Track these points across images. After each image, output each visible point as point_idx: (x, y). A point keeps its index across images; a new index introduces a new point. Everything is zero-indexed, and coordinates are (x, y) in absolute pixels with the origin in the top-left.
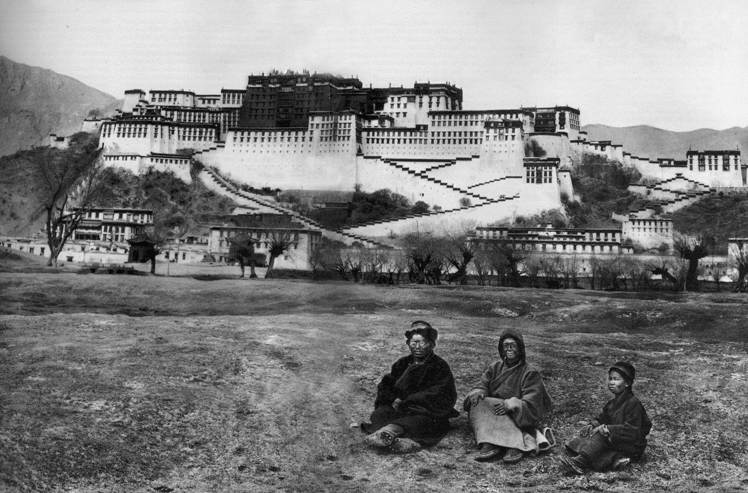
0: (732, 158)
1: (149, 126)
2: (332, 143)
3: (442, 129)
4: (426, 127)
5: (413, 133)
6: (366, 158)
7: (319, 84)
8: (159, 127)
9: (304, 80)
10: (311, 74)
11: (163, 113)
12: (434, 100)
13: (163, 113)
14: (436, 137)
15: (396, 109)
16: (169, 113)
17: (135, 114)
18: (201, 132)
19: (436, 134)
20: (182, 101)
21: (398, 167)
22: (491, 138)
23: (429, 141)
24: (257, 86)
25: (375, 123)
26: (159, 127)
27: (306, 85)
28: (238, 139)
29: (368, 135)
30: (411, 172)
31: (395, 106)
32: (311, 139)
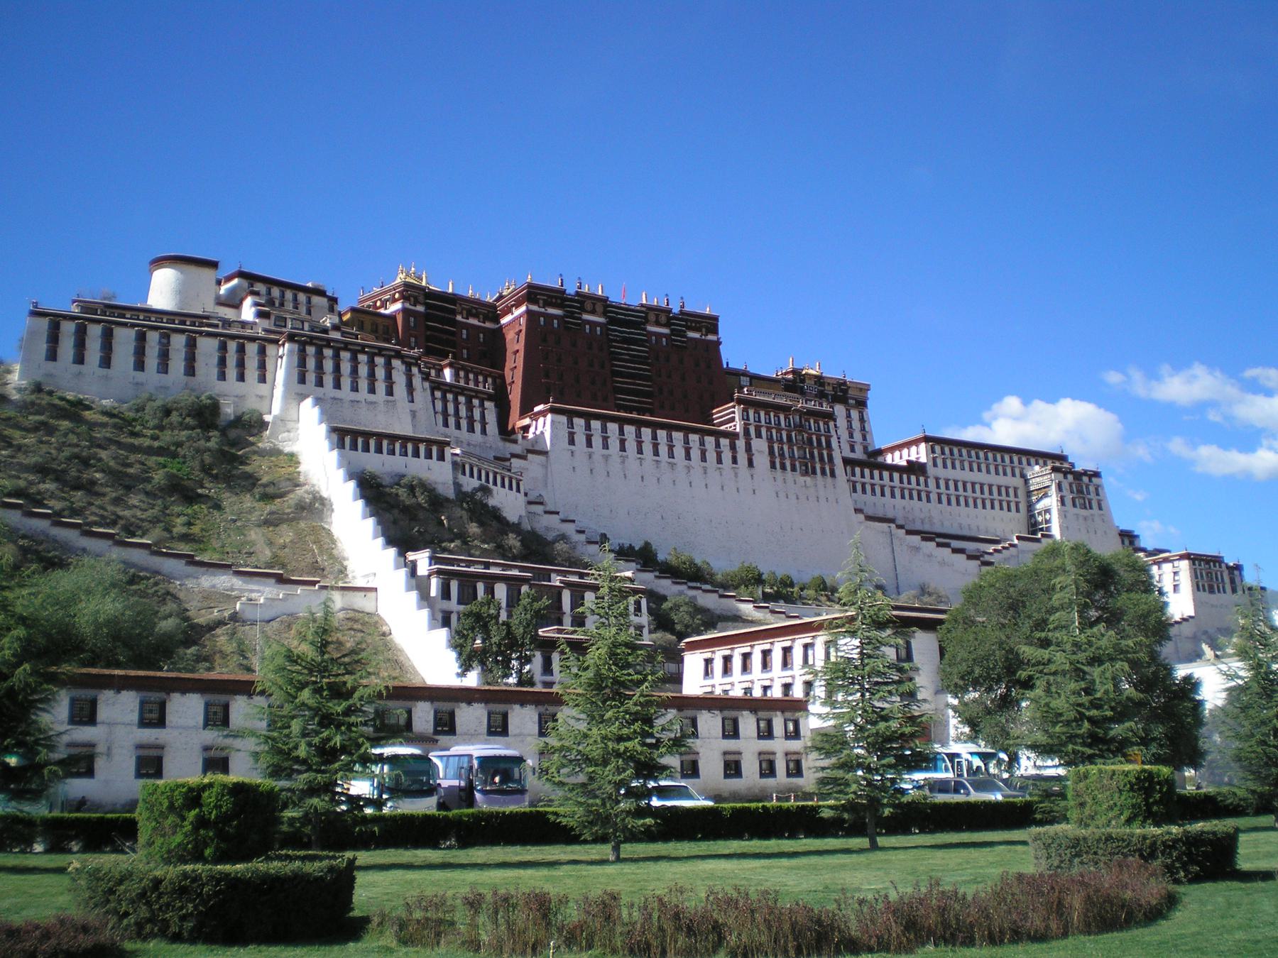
0: (1236, 572)
1: (396, 363)
3: (950, 473)
5: (905, 477)
6: (869, 518)
7: (696, 335)
9: (663, 319)
10: (676, 310)
12: (855, 414)
18: (470, 408)
21: (939, 545)
23: (934, 497)
24: (551, 311)
27: (666, 331)
28: (580, 438)
30: (970, 557)
32: (751, 464)
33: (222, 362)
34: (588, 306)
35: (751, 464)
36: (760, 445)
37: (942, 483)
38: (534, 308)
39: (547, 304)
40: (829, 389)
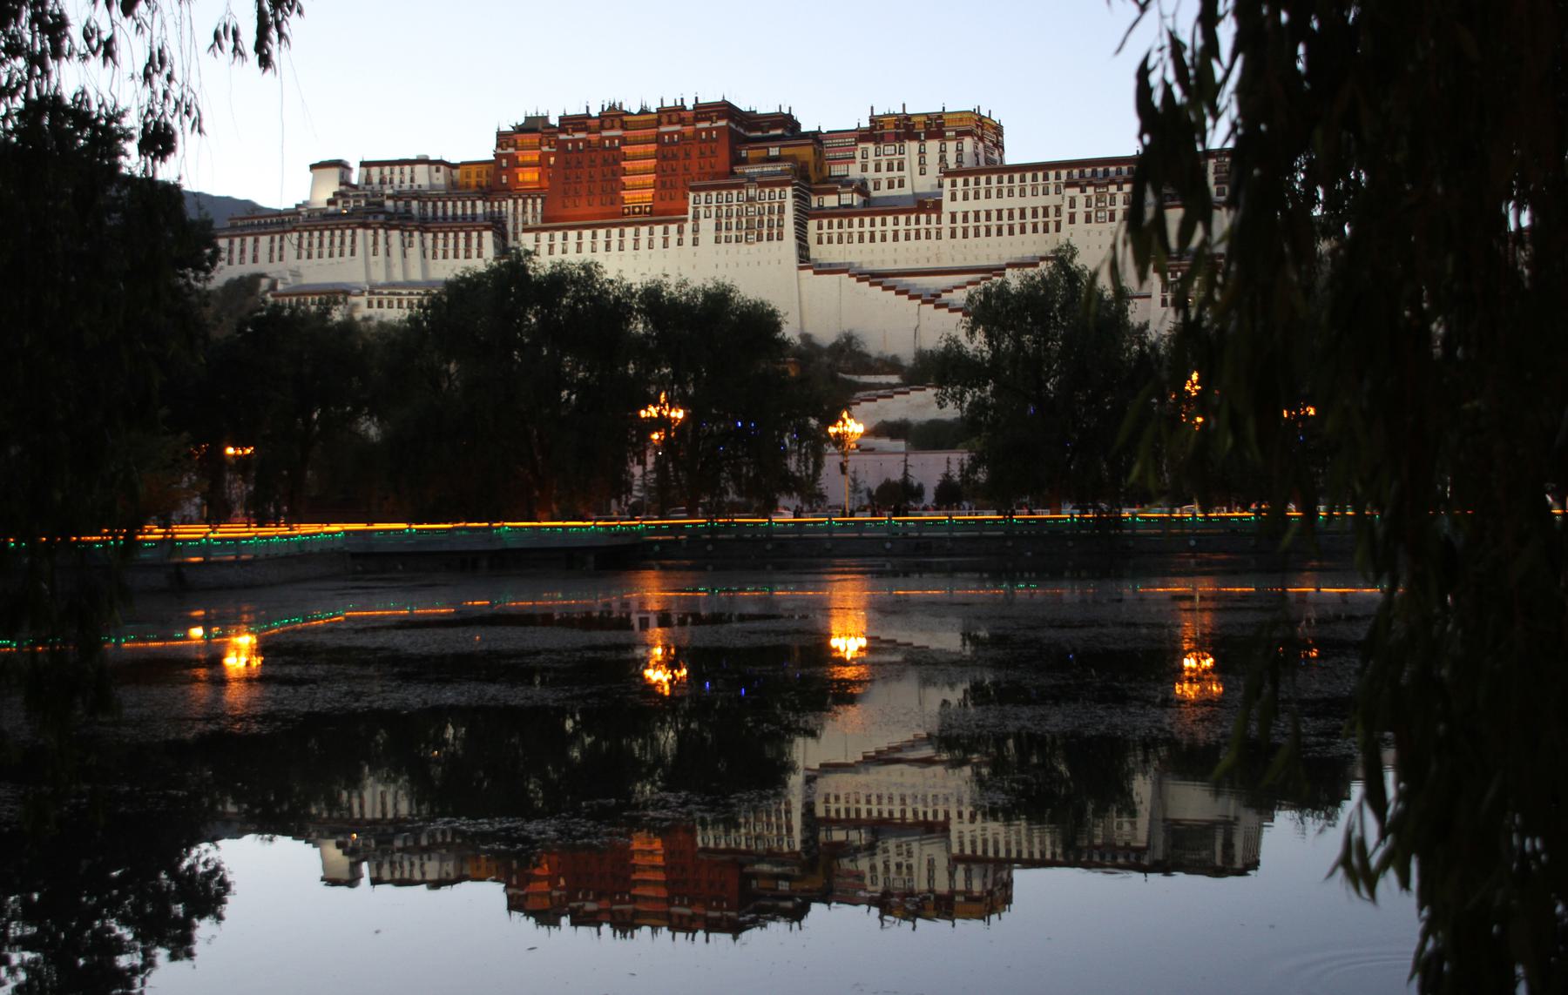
1: (359, 231)
2: (743, 246)
3: (972, 205)
4: (937, 207)
7: (706, 125)
8: (381, 232)
9: (675, 118)
10: (689, 105)
11: (389, 204)
12: (951, 146)
13: (389, 204)
14: (959, 223)
15: (871, 174)
16: (401, 204)
17: (332, 208)
19: (959, 217)
20: (422, 176)
21: (885, 289)
22: (1080, 218)
23: (946, 233)
25: (831, 201)
26: (381, 232)
29: (820, 227)
30: (912, 298)
31: (871, 167)
32: (695, 242)
33: (272, 250)
34: (607, 123)
35: (695, 242)
36: (707, 226)
37: (959, 217)
38: (563, 137)
39: (575, 130)
40: (920, 129)
